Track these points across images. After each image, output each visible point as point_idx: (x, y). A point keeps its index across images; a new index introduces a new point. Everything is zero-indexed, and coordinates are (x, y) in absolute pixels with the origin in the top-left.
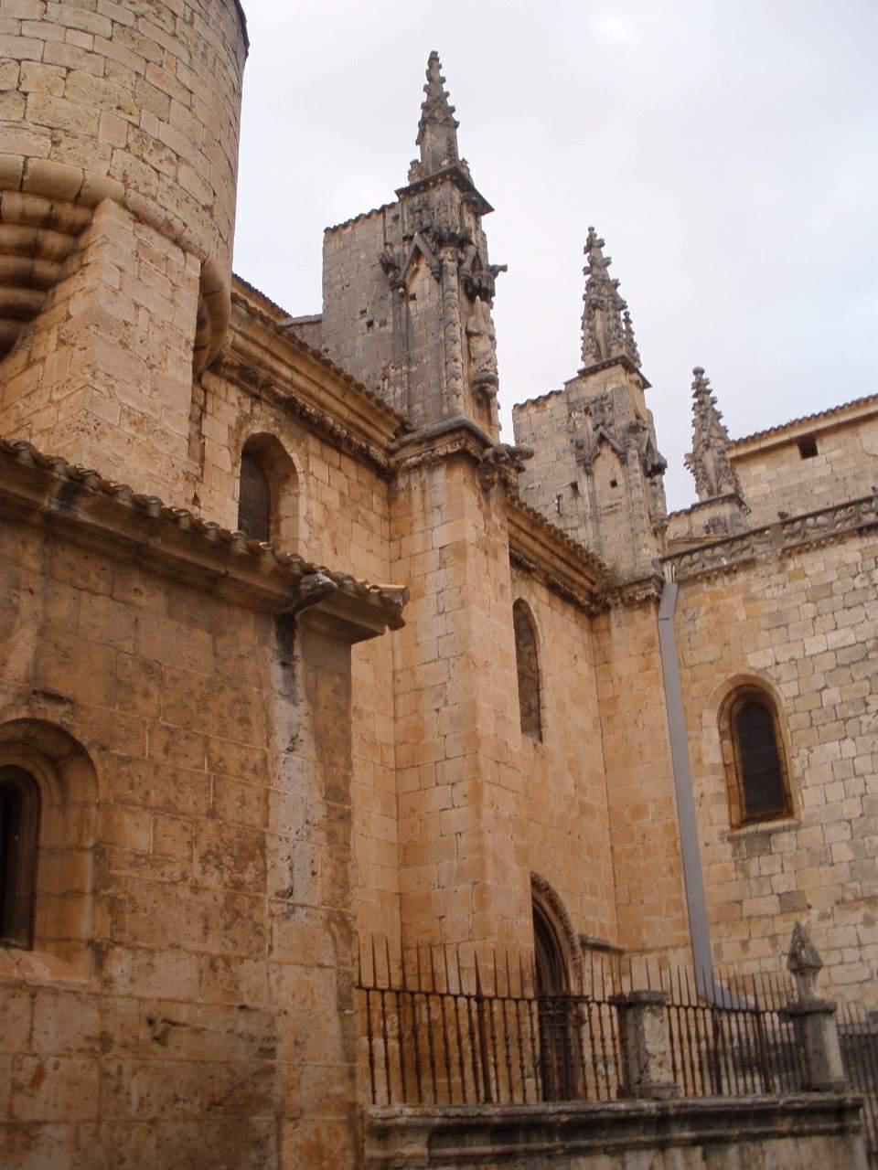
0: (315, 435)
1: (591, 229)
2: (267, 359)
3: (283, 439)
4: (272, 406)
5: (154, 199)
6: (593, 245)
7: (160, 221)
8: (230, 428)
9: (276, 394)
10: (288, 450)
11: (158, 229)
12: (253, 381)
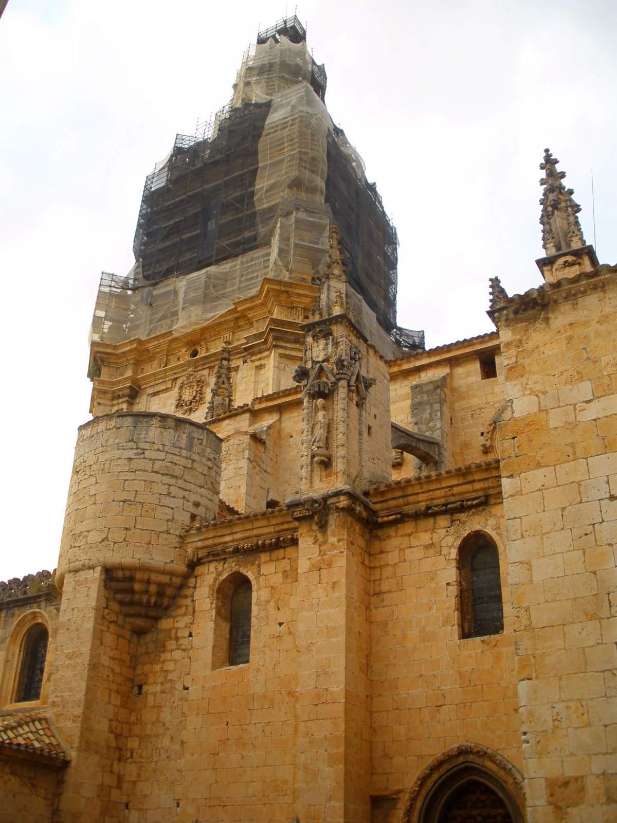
0: (261, 552)
1: (547, 151)
2: (217, 541)
3: (243, 571)
4: (233, 557)
5: (77, 560)
6: (549, 162)
7: (81, 567)
8: (210, 586)
9: (230, 552)
10: (245, 573)
11: (82, 570)
12: (218, 555)
